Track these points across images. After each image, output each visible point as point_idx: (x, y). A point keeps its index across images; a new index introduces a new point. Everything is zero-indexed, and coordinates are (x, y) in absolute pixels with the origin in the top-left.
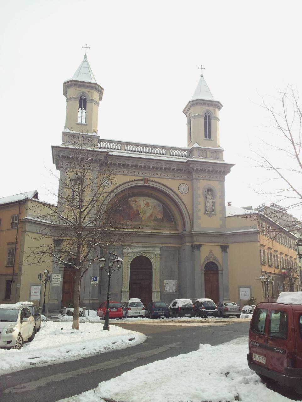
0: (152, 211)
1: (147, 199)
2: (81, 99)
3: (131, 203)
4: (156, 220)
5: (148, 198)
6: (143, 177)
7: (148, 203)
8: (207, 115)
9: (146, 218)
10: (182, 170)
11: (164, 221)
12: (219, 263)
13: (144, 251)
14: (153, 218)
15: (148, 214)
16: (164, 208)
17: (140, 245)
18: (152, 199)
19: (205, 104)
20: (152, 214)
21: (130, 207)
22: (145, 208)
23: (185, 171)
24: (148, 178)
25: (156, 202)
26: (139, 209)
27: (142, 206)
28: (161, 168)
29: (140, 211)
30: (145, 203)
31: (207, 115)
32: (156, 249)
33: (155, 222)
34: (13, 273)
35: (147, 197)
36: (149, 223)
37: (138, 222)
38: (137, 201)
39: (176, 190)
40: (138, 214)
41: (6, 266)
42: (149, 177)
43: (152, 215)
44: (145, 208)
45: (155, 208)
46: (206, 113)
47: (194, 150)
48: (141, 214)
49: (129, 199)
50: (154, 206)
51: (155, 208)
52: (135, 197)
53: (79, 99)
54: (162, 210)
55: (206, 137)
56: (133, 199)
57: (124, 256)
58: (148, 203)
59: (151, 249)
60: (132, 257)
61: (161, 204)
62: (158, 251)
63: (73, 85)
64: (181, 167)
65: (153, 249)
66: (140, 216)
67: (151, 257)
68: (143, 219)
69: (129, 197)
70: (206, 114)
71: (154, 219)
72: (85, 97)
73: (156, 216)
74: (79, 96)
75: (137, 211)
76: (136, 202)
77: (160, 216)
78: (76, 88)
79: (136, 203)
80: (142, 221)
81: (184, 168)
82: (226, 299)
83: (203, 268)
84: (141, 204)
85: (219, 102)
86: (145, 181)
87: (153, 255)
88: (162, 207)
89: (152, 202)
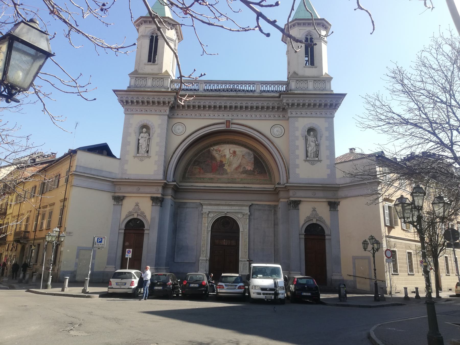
0: (239, 161)
1: (234, 148)
2: (152, 37)
3: (214, 153)
4: (245, 172)
5: (234, 146)
6: (224, 119)
7: (235, 152)
8: (309, 38)
9: (232, 170)
10: (273, 108)
11: (256, 173)
12: (147, 221)
13: (228, 211)
14: (241, 170)
15: (235, 166)
16: (255, 158)
17: (223, 202)
18: (240, 147)
19: (304, 24)
20: (239, 165)
21: (213, 158)
22: (232, 158)
23: (278, 108)
24: (231, 120)
25: (245, 150)
26: (223, 159)
27: (228, 156)
28: (246, 108)
29: (224, 162)
30: (231, 152)
31: (309, 38)
32: (244, 208)
33: (244, 175)
34: (35, 237)
35: (234, 144)
36: (236, 176)
37: (222, 174)
38: (221, 150)
39: (267, 133)
40: (222, 165)
41: (39, 230)
42: (232, 119)
43: (239, 166)
44: (232, 158)
45: (244, 158)
46: (307, 36)
47: (291, 81)
48: (226, 165)
49: (212, 148)
50: (243, 156)
51: (244, 158)
52: (218, 146)
53: (149, 37)
54: (253, 160)
55: (149, 60)
56: (216, 148)
57: (203, 216)
58: (235, 152)
59: (237, 208)
60: (213, 217)
61: (251, 152)
62: (246, 210)
63: (143, 22)
64: (273, 104)
65: (240, 208)
66: (224, 167)
67: (238, 218)
68: (229, 171)
69: (211, 146)
70: (308, 37)
71: (243, 171)
72: (156, 34)
73: (244, 168)
74: (149, 34)
75: (221, 162)
76: (220, 151)
77: (250, 167)
78: (146, 25)
79: (219, 152)
80: (227, 174)
81: (276, 105)
82: (294, 272)
83: (123, 227)
84: (226, 154)
85: (323, 19)
86: (226, 124)
87: (240, 216)
88: (252, 156)
89: (240, 150)
